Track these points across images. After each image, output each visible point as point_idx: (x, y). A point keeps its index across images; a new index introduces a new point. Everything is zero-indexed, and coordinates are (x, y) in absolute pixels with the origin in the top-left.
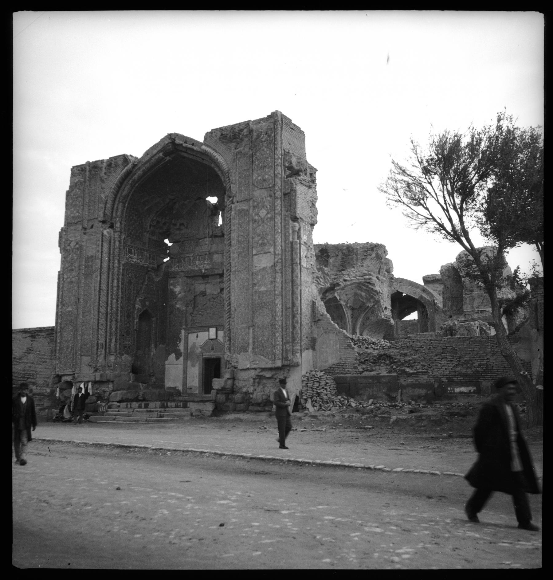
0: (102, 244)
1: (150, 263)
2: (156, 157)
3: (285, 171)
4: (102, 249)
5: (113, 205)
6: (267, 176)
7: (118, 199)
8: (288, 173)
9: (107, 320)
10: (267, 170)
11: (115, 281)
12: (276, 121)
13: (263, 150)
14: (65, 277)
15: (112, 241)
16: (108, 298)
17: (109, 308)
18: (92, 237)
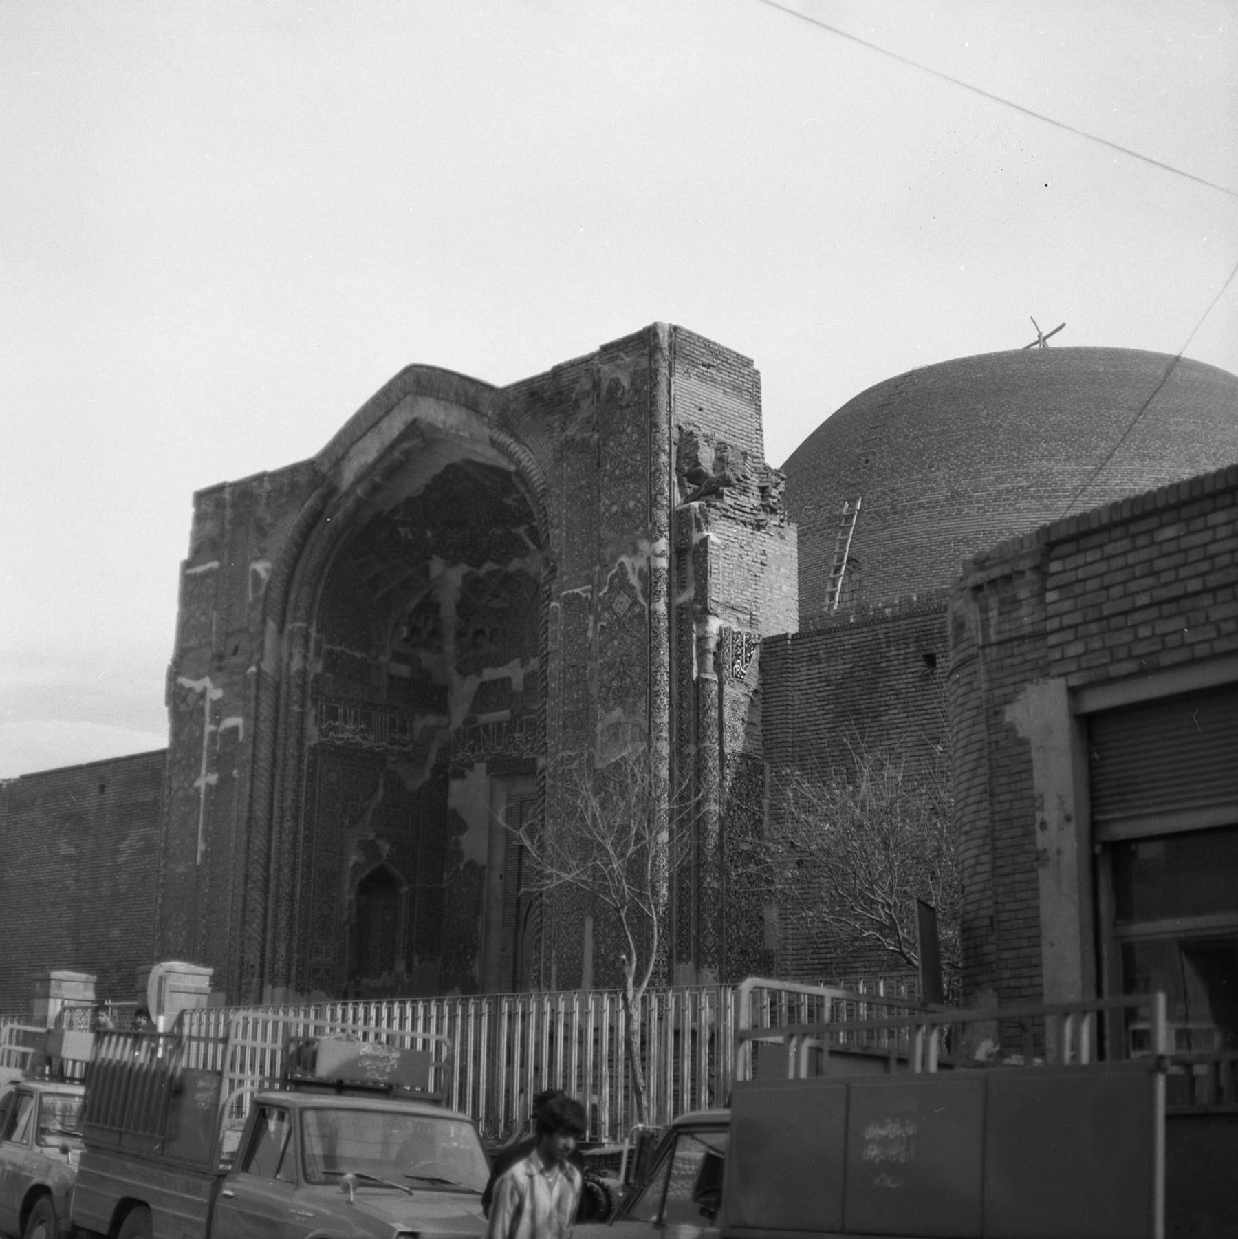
0: (257, 698)
1: (392, 743)
2: (386, 464)
3: (681, 485)
4: (257, 711)
5: (287, 593)
6: (632, 504)
7: (298, 576)
8: (689, 491)
9: (266, 899)
10: (632, 486)
11: (290, 795)
12: (645, 355)
13: (624, 431)
14: (175, 785)
15: (284, 688)
16: (269, 841)
17: (273, 866)
18: (235, 677)
